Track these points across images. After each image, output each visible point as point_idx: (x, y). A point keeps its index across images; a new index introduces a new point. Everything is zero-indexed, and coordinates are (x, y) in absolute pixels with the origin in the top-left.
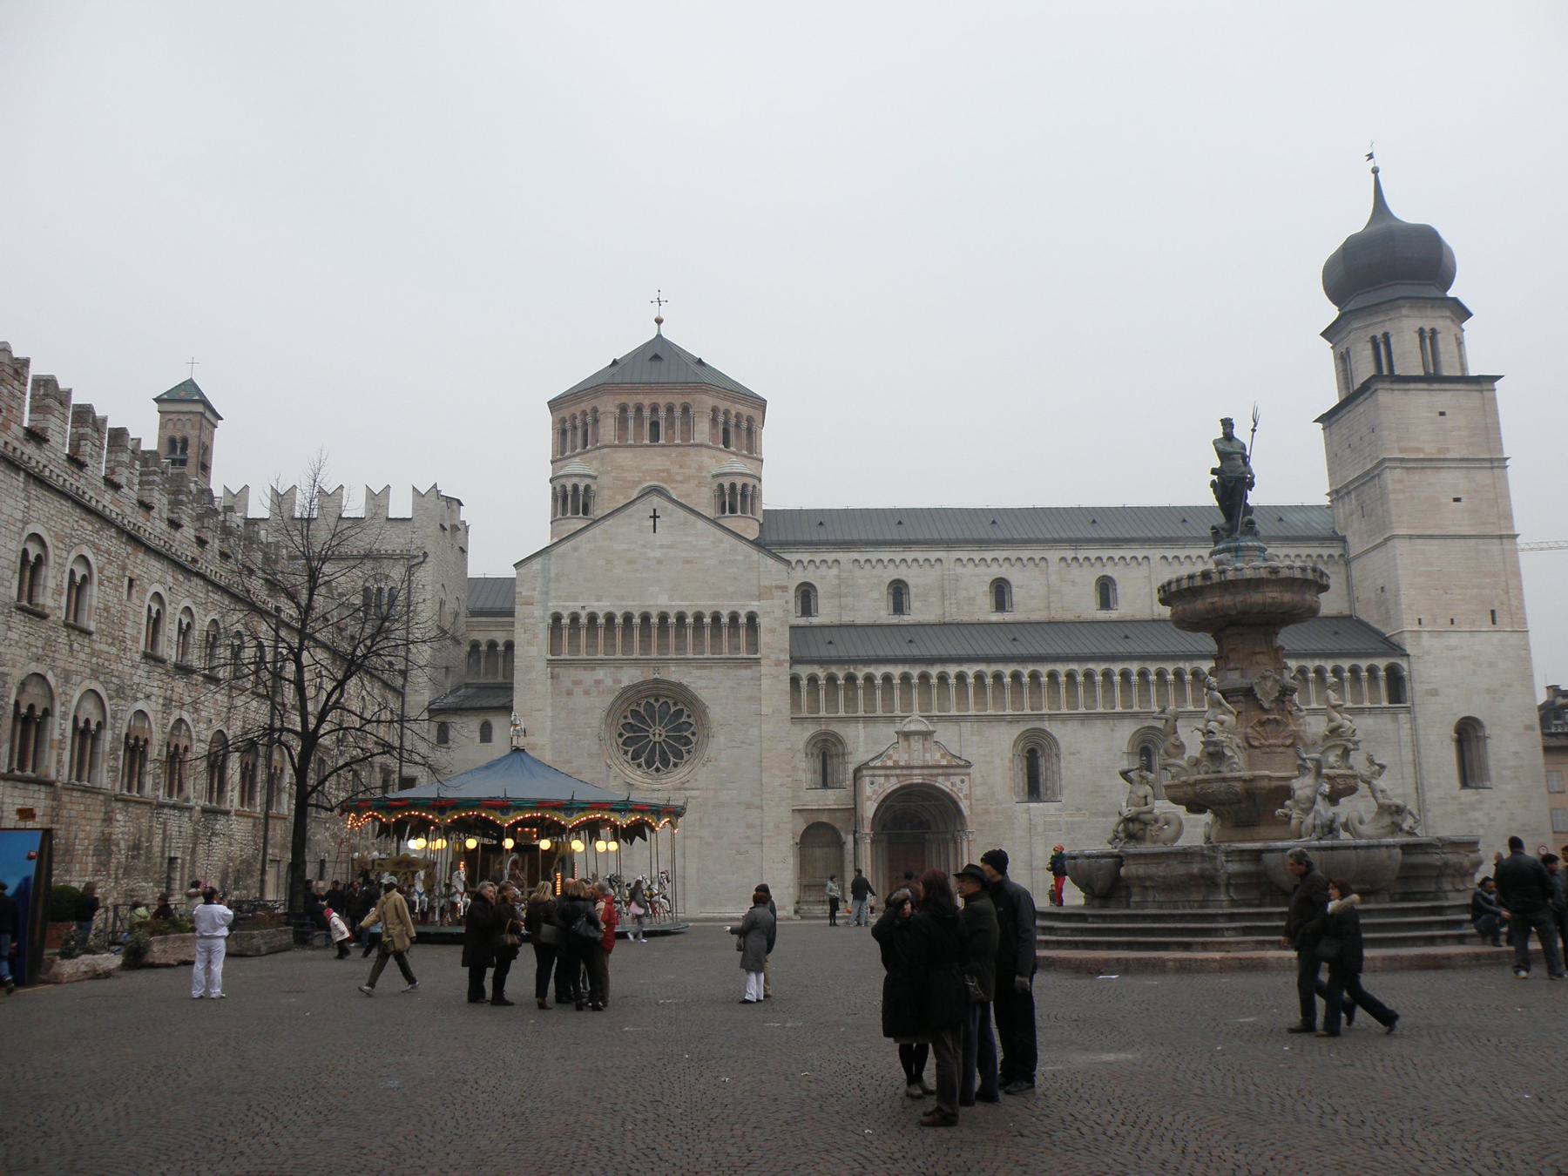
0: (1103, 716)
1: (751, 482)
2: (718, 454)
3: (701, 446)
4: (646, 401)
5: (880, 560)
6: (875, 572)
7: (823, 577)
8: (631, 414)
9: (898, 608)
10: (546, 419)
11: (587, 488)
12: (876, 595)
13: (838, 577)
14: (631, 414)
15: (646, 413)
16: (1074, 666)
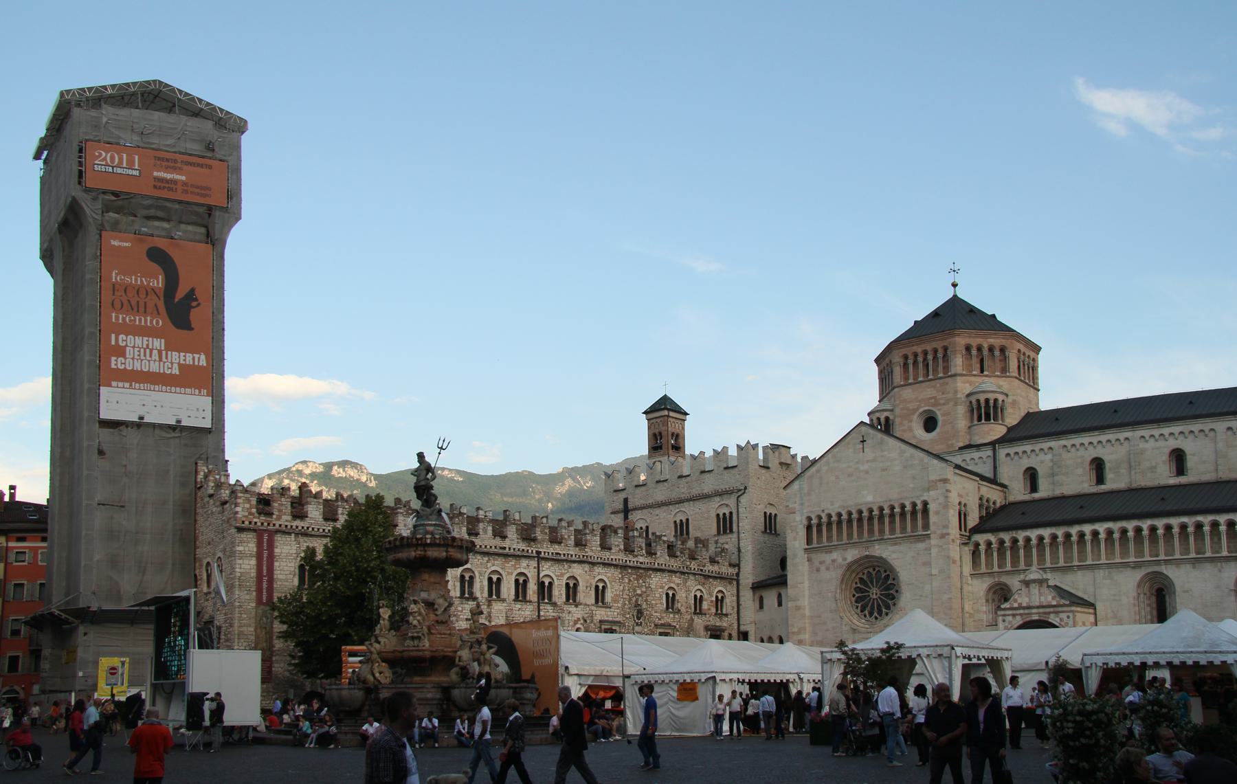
0: (1211, 560)
1: (991, 396)
2: (973, 379)
3: (955, 375)
4: (919, 350)
5: (1082, 444)
6: (1079, 454)
7: (1042, 462)
8: (910, 361)
9: (1100, 480)
10: (875, 369)
11: (887, 419)
12: (1079, 471)
13: (1052, 460)
14: (910, 361)
15: (920, 359)
16: (1185, 519)
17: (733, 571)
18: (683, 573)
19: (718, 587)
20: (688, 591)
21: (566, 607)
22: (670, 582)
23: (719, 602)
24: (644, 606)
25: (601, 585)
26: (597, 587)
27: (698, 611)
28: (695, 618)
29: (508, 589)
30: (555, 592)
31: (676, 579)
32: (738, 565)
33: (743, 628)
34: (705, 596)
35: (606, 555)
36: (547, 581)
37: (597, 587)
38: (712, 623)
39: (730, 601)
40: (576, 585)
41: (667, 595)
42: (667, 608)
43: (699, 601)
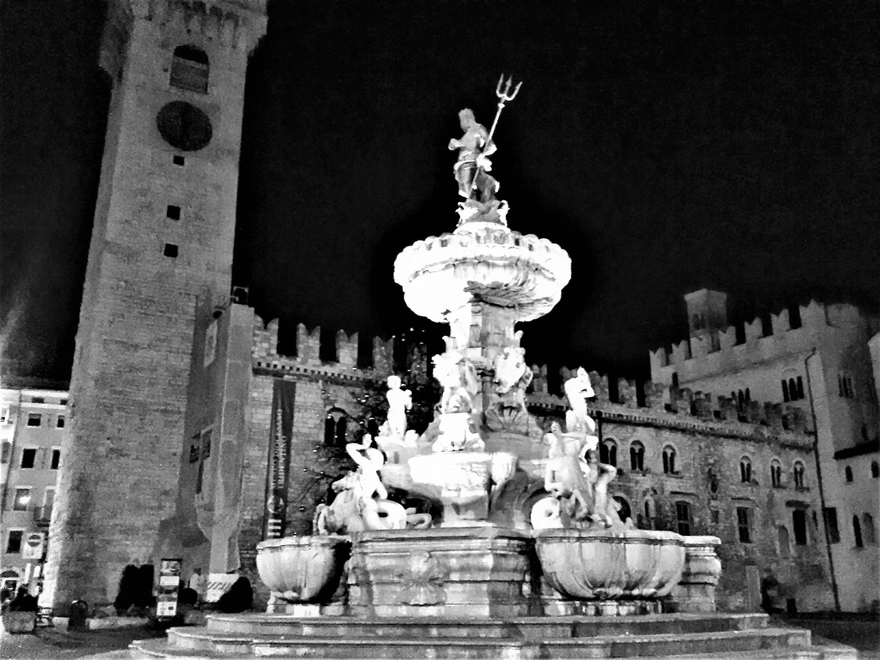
17: (809, 440)
18: (758, 441)
19: (795, 457)
20: (764, 461)
21: (632, 476)
22: (744, 450)
23: (798, 474)
24: (718, 477)
25: (669, 452)
26: (665, 454)
27: (777, 484)
28: (775, 491)
30: (620, 458)
31: (750, 447)
32: (814, 433)
33: (828, 505)
34: (783, 467)
35: (672, 419)
36: (610, 445)
37: (665, 454)
38: (795, 498)
39: (810, 474)
40: (642, 451)
41: (742, 465)
42: (744, 480)
43: (776, 473)
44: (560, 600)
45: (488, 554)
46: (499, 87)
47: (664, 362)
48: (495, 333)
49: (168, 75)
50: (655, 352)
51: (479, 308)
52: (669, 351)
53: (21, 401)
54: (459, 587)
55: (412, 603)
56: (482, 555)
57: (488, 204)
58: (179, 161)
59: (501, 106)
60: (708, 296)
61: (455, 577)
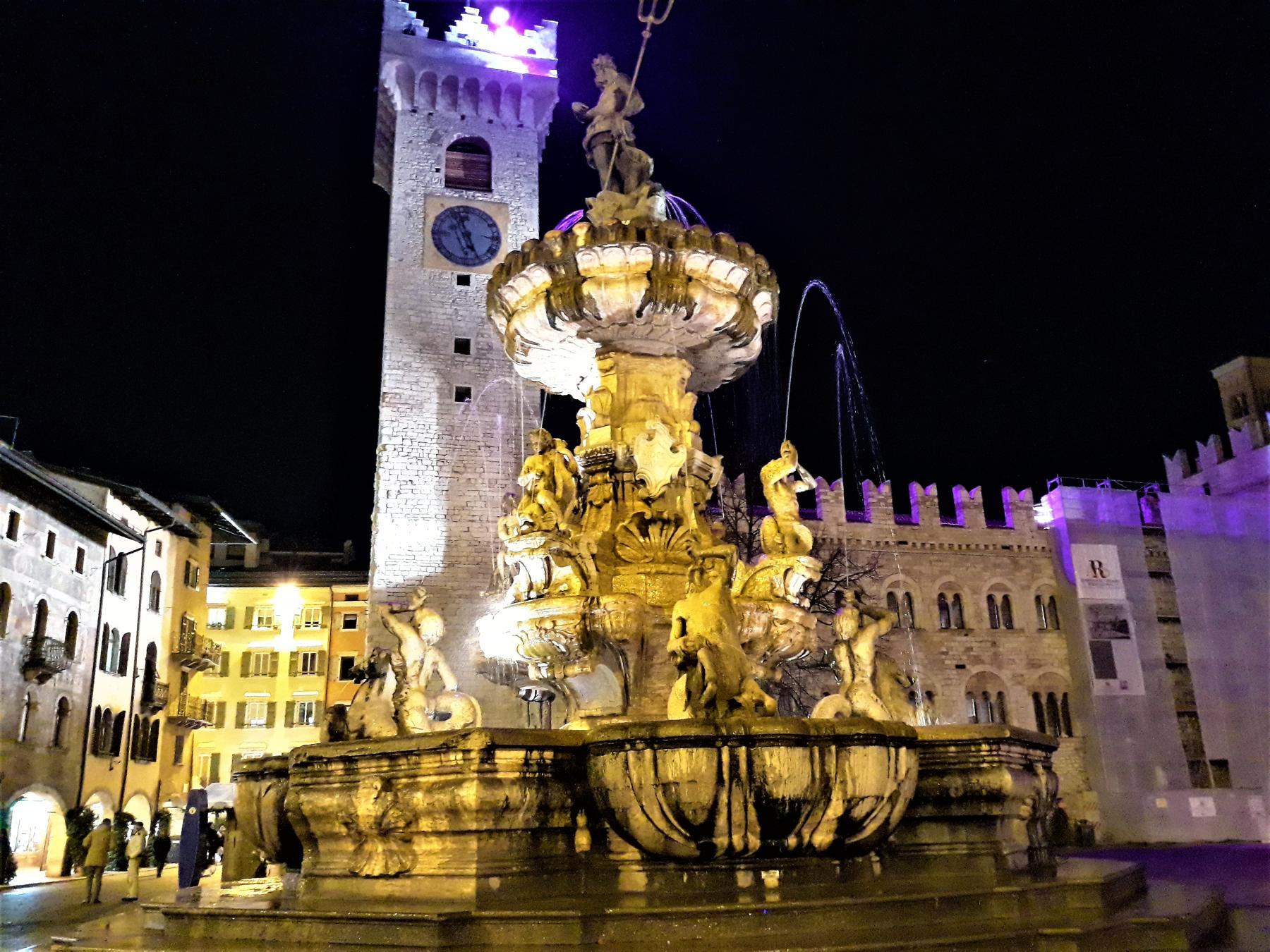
29: (1025, 612)
44: (638, 862)
45: (473, 780)
46: (640, 10)
47: (1189, 469)
48: (639, 400)
49: (441, 175)
50: (1171, 456)
51: (608, 363)
52: (1192, 456)
53: (332, 600)
54: (435, 844)
55: (363, 874)
56: (459, 783)
57: (634, 194)
58: (464, 280)
59: (646, 34)
60: (1249, 366)
61: (425, 824)
